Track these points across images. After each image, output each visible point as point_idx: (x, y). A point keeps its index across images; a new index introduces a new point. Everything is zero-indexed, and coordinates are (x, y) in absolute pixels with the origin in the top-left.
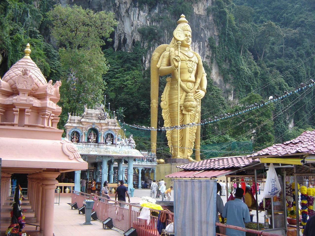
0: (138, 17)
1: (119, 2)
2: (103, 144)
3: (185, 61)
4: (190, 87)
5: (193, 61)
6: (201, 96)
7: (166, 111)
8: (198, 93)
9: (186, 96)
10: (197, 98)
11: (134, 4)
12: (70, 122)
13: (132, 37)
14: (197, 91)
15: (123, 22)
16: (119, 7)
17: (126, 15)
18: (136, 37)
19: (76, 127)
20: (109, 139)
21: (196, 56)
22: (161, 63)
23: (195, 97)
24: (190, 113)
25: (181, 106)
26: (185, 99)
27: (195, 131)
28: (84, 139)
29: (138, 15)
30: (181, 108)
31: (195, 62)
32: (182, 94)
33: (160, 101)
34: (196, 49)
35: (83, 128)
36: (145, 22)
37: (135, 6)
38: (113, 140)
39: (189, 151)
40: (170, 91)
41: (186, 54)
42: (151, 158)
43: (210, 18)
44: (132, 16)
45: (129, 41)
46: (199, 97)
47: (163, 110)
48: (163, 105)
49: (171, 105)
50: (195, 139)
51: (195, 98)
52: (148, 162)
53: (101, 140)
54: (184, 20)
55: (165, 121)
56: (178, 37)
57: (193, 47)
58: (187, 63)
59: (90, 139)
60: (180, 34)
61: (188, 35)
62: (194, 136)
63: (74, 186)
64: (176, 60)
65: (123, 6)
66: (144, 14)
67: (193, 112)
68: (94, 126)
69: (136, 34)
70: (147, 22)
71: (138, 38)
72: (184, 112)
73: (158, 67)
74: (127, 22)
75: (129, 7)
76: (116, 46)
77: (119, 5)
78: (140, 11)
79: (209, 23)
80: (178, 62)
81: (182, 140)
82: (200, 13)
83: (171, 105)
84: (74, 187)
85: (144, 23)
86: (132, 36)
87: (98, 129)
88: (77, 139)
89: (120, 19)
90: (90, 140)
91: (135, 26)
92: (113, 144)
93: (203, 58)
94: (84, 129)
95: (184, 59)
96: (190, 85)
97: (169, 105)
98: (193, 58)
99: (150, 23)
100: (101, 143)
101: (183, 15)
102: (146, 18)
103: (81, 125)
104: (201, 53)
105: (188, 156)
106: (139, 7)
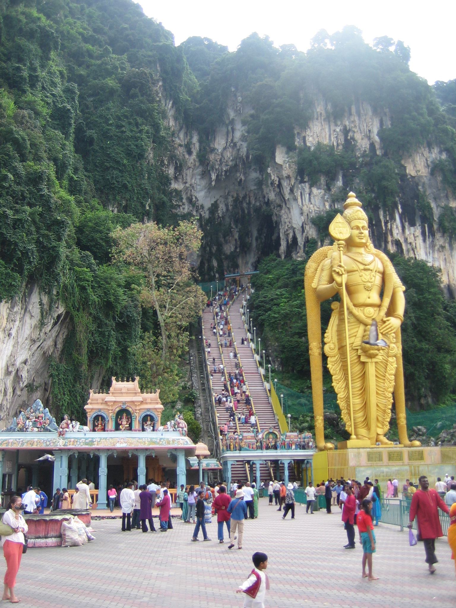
0: (310, 199)
1: (278, 177)
2: (139, 431)
3: (357, 272)
4: (371, 315)
6: (392, 328)
7: (334, 359)
8: (386, 324)
9: (365, 331)
11: (301, 177)
12: (91, 403)
13: (302, 234)
14: (385, 319)
15: (289, 209)
16: (280, 185)
17: (291, 197)
18: (310, 233)
19: (100, 410)
20: (149, 423)
21: (381, 259)
22: (319, 280)
23: (381, 331)
24: (374, 360)
25: (357, 349)
26: (364, 336)
27: (391, 390)
28: (111, 425)
29: (310, 194)
30: (357, 351)
33: (323, 343)
34: (417, 239)
35: (109, 410)
36: (322, 204)
37: (302, 181)
38: (154, 424)
39: (380, 425)
40: (339, 325)
41: (359, 259)
42: (303, 443)
43: (438, 178)
44: (299, 198)
45: (301, 241)
46: (390, 329)
47: (329, 359)
48: (329, 350)
49: (342, 348)
50: (394, 405)
52: (299, 450)
53: (136, 425)
54: (352, 201)
55: (333, 377)
56: (338, 234)
57: (412, 236)
58: (361, 274)
59: (121, 424)
60: (341, 229)
61: (360, 225)
62: (390, 398)
63: (97, 493)
64: (338, 273)
65: (285, 184)
66: (319, 191)
67: (381, 357)
68: (124, 407)
69: (310, 228)
70: (324, 204)
71: (312, 232)
72: (363, 359)
73: (315, 287)
74: (294, 209)
75: (295, 183)
76: (283, 251)
77: (279, 182)
79: (438, 188)
80: (341, 275)
82: (420, 174)
83: (342, 348)
84: (97, 496)
85: (322, 208)
86: (303, 231)
87: (130, 410)
88: (102, 425)
89: (284, 206)
90: (121, 427)
91: (306, 214)
92: (153, 430)
93: (433, 251)
94: (111, 411)
95: (356, 268)
96: (371, 310)
97: (339, 349)
98: (373, 264)
99: (330, 206)
100: (136, 431)
101: (351, 193)
102: (323, 198)
103: (107, 407)
104: (428, 242)
105: (378, 434)
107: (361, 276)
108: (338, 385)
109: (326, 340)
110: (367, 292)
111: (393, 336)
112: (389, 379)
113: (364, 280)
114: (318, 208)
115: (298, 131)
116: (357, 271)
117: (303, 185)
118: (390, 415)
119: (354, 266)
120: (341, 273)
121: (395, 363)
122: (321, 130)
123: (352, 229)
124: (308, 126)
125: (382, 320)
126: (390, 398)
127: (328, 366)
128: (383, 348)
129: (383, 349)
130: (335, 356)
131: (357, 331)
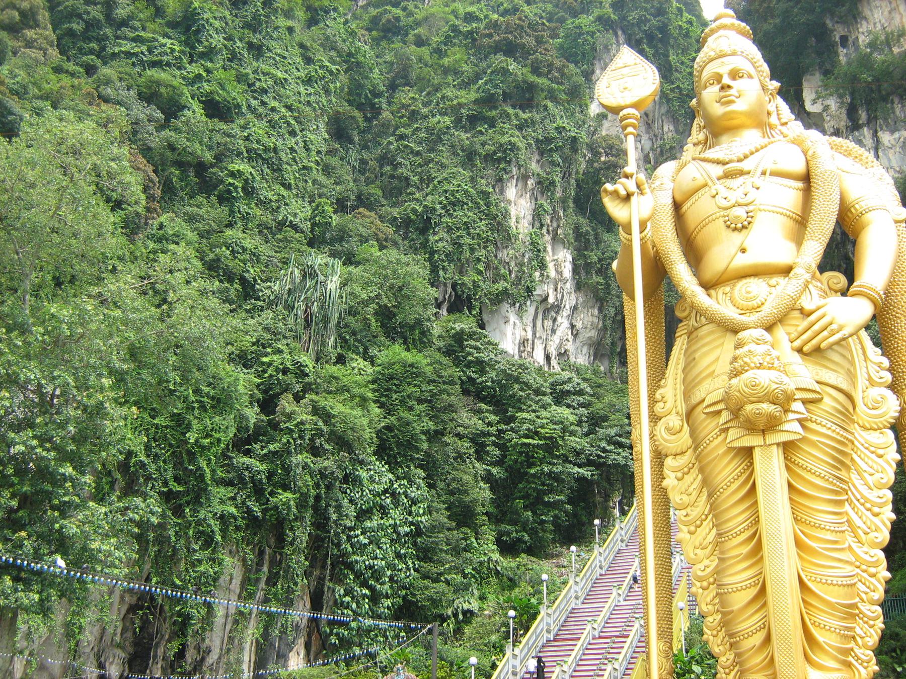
3: (707, 189)
4: (754, 303)
5: (746, 169)
6: (834, 327)
10: (814, 342)
23: (797, 344)
31: (764, 173)
32: (718, 351)
46: (825, 333)
47: (669, 462)
51: (800, 351)
61: (724, 70)
66: (897, 135)
67: (796, 427)
78: (880, 134)
81: (765, 604)
95: (700, 181)
96: (756, 287)
106: (870, 121)
107: (714, 197)
108: (693, 536)
109: (658, 408)
110: (736, 232)
111: (879, 365)
112: (867, 500)
113: (725, 204)
114: (899, 172)
115: (842, 33)
116: (706, 185)
117: (857, 133)
118: (880, 624)
119: (698, 176)
120: (623, 193)
121: (894, 446)
122: (890, 12)
123: (706, 87)
124: (859, 13)
125: (802, 310)
126: (876, 564)
127: (665, 483)
128: (799, 395)
129: (805, 402)
130: (683, 453)
131: (717, 359)
